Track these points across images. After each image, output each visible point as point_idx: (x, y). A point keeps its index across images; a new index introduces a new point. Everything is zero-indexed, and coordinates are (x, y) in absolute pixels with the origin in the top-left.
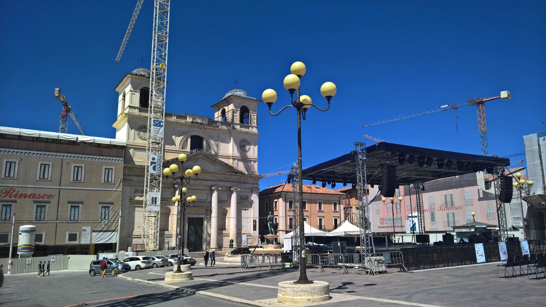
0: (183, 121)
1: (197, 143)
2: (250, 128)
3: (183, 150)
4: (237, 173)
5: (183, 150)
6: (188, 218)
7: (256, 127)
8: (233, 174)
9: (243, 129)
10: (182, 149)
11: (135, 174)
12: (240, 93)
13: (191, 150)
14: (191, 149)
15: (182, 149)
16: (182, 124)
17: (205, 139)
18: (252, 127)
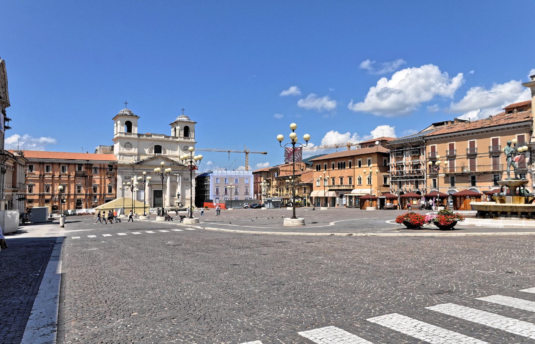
0: (149, 138)
1: (158, 149)
2: (190, 140)
3: (151, 154)
4: (181, 166)
5: (151, 154)
6: (154, 191)
7: (194, 138)
8: (179, 166)
9: (186, 140)
10: (150, 153)
11: (124, 168)
12: (185, 119)
13: (155, 153)
14: (155, 153)
15: (150, 153)
16: (149, 140)
17: (162, 148)
18: (192, 138)
